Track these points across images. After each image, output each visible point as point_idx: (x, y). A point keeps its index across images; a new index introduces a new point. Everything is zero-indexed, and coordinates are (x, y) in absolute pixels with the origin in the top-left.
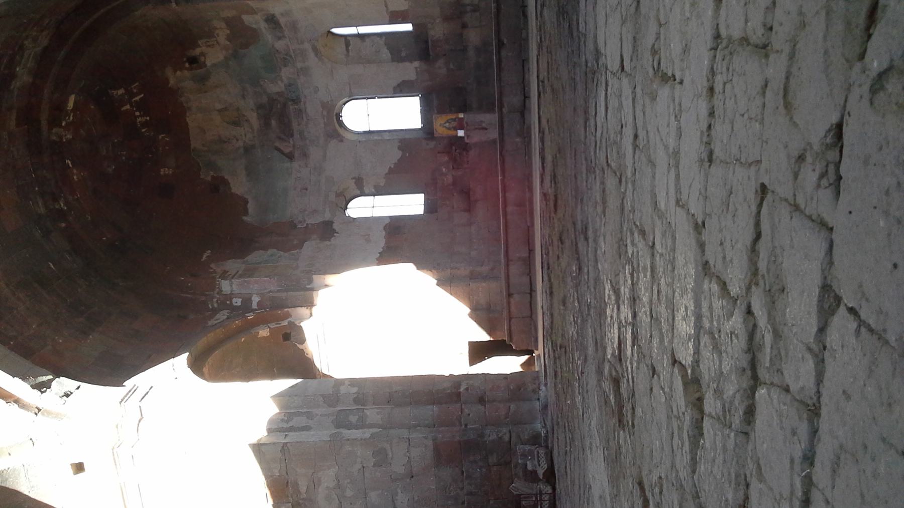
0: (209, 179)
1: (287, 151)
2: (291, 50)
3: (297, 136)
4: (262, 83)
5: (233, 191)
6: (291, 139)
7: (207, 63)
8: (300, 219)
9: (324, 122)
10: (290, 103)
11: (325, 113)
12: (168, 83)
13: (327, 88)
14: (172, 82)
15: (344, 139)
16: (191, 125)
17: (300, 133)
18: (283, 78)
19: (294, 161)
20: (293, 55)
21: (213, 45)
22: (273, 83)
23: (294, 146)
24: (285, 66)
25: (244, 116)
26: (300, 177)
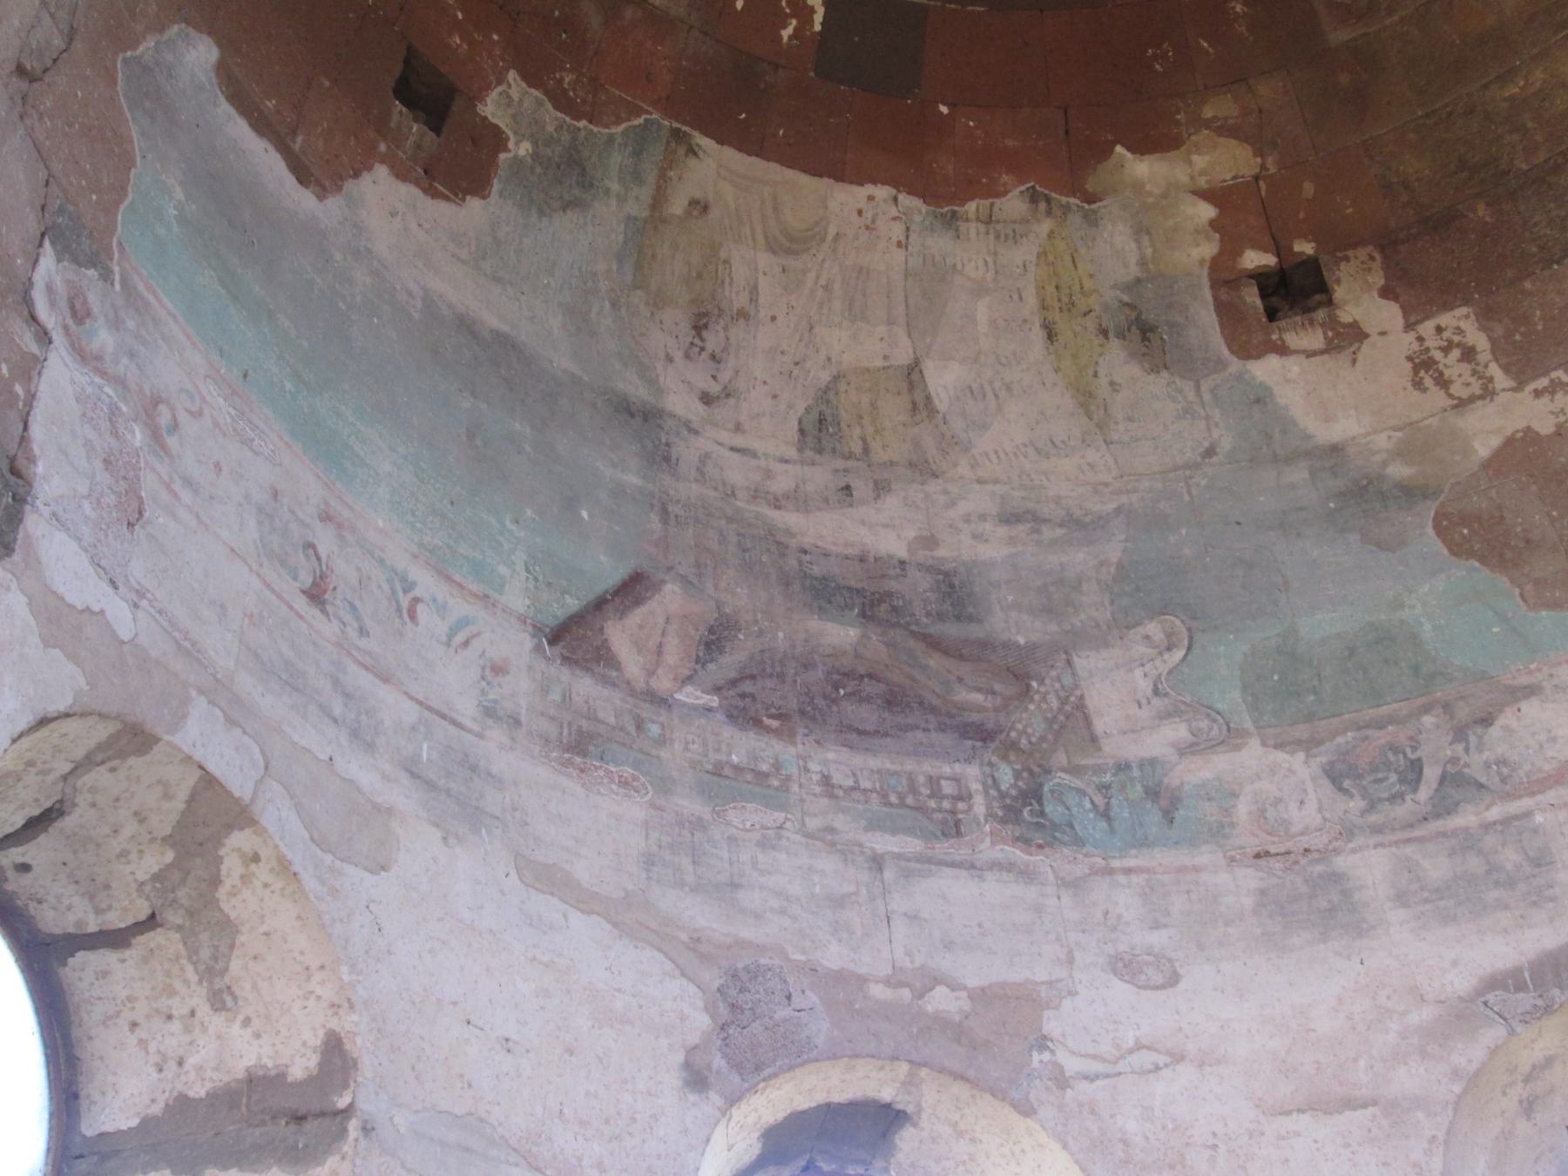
0: (491, 109)
1: (620, 635)
2: (1515, 807)
3: (742, 746)
4: (1153, 629)
5: (381, 171)
6: (714, 701)
7: (1273, 361)
8: (103, 338)
9: (863, 980)
10: (1006, 775)
11: (942, 1001)
12: (1142, 147)
13: (1178, 1058)
14: (1141, 168)
15: (715, 1098)
16: (846, 199)
17: (761, 776)
18: (1220, 764)
19: (538, 648)
20: (1466, 818)
21: (1443, 383)
22: (1156, 692)
23: (662, 702)
24: (1336, 776)
25: (881, 488)
26: (412, 615)
